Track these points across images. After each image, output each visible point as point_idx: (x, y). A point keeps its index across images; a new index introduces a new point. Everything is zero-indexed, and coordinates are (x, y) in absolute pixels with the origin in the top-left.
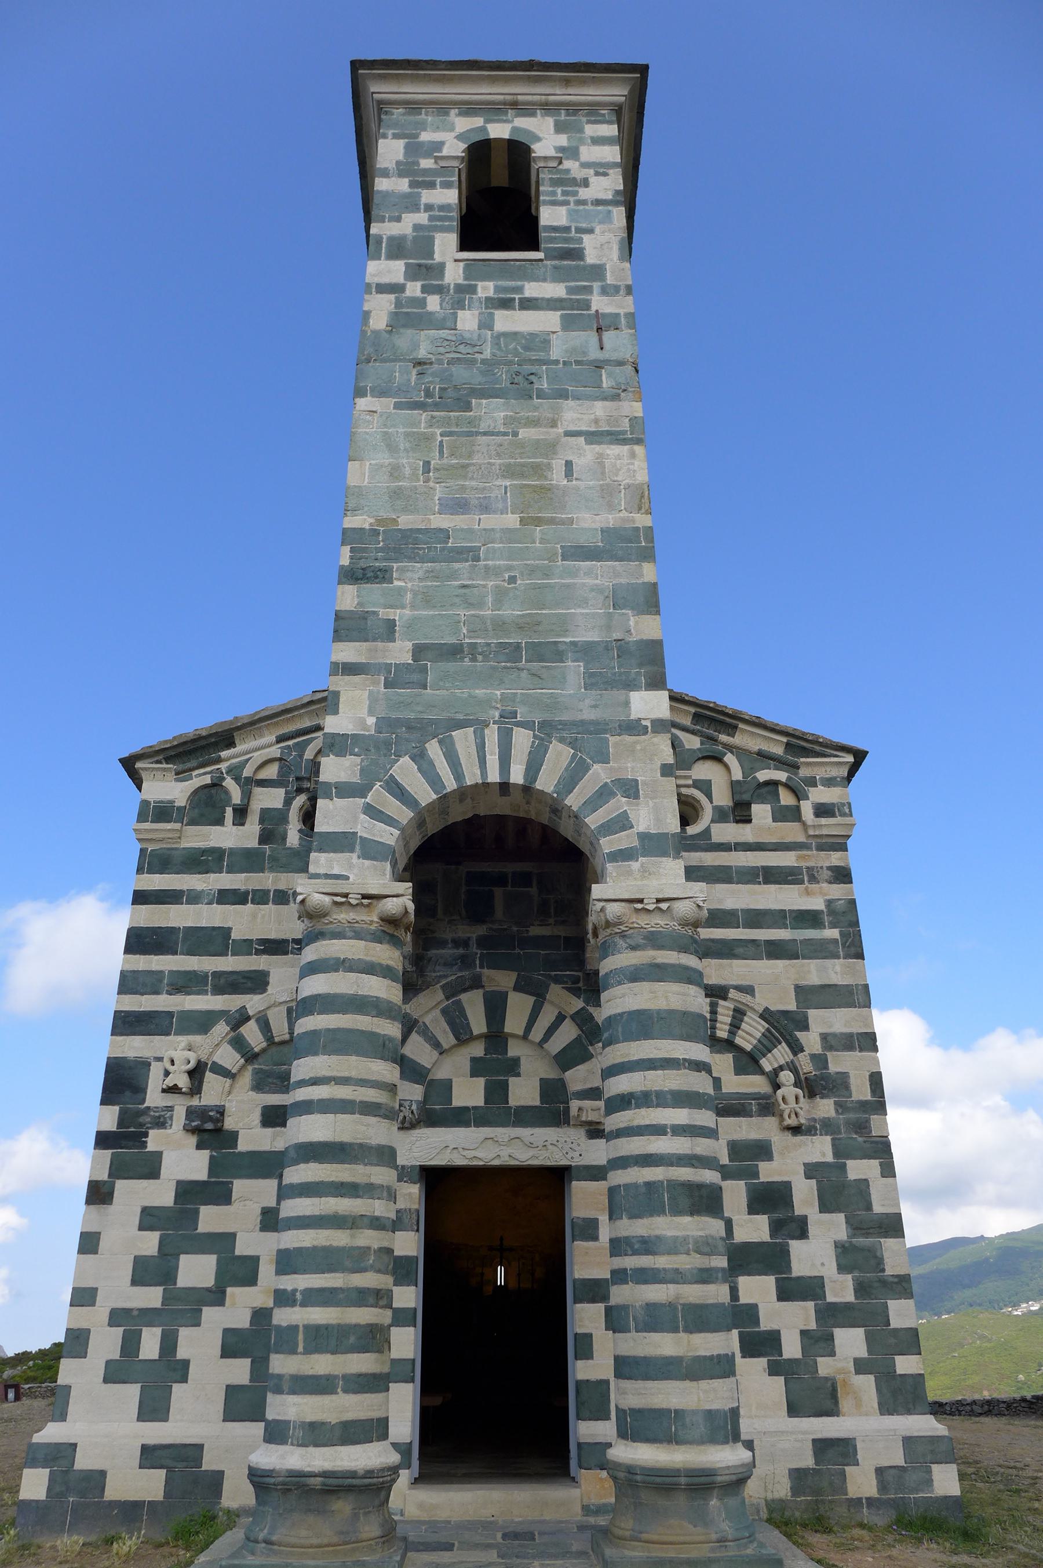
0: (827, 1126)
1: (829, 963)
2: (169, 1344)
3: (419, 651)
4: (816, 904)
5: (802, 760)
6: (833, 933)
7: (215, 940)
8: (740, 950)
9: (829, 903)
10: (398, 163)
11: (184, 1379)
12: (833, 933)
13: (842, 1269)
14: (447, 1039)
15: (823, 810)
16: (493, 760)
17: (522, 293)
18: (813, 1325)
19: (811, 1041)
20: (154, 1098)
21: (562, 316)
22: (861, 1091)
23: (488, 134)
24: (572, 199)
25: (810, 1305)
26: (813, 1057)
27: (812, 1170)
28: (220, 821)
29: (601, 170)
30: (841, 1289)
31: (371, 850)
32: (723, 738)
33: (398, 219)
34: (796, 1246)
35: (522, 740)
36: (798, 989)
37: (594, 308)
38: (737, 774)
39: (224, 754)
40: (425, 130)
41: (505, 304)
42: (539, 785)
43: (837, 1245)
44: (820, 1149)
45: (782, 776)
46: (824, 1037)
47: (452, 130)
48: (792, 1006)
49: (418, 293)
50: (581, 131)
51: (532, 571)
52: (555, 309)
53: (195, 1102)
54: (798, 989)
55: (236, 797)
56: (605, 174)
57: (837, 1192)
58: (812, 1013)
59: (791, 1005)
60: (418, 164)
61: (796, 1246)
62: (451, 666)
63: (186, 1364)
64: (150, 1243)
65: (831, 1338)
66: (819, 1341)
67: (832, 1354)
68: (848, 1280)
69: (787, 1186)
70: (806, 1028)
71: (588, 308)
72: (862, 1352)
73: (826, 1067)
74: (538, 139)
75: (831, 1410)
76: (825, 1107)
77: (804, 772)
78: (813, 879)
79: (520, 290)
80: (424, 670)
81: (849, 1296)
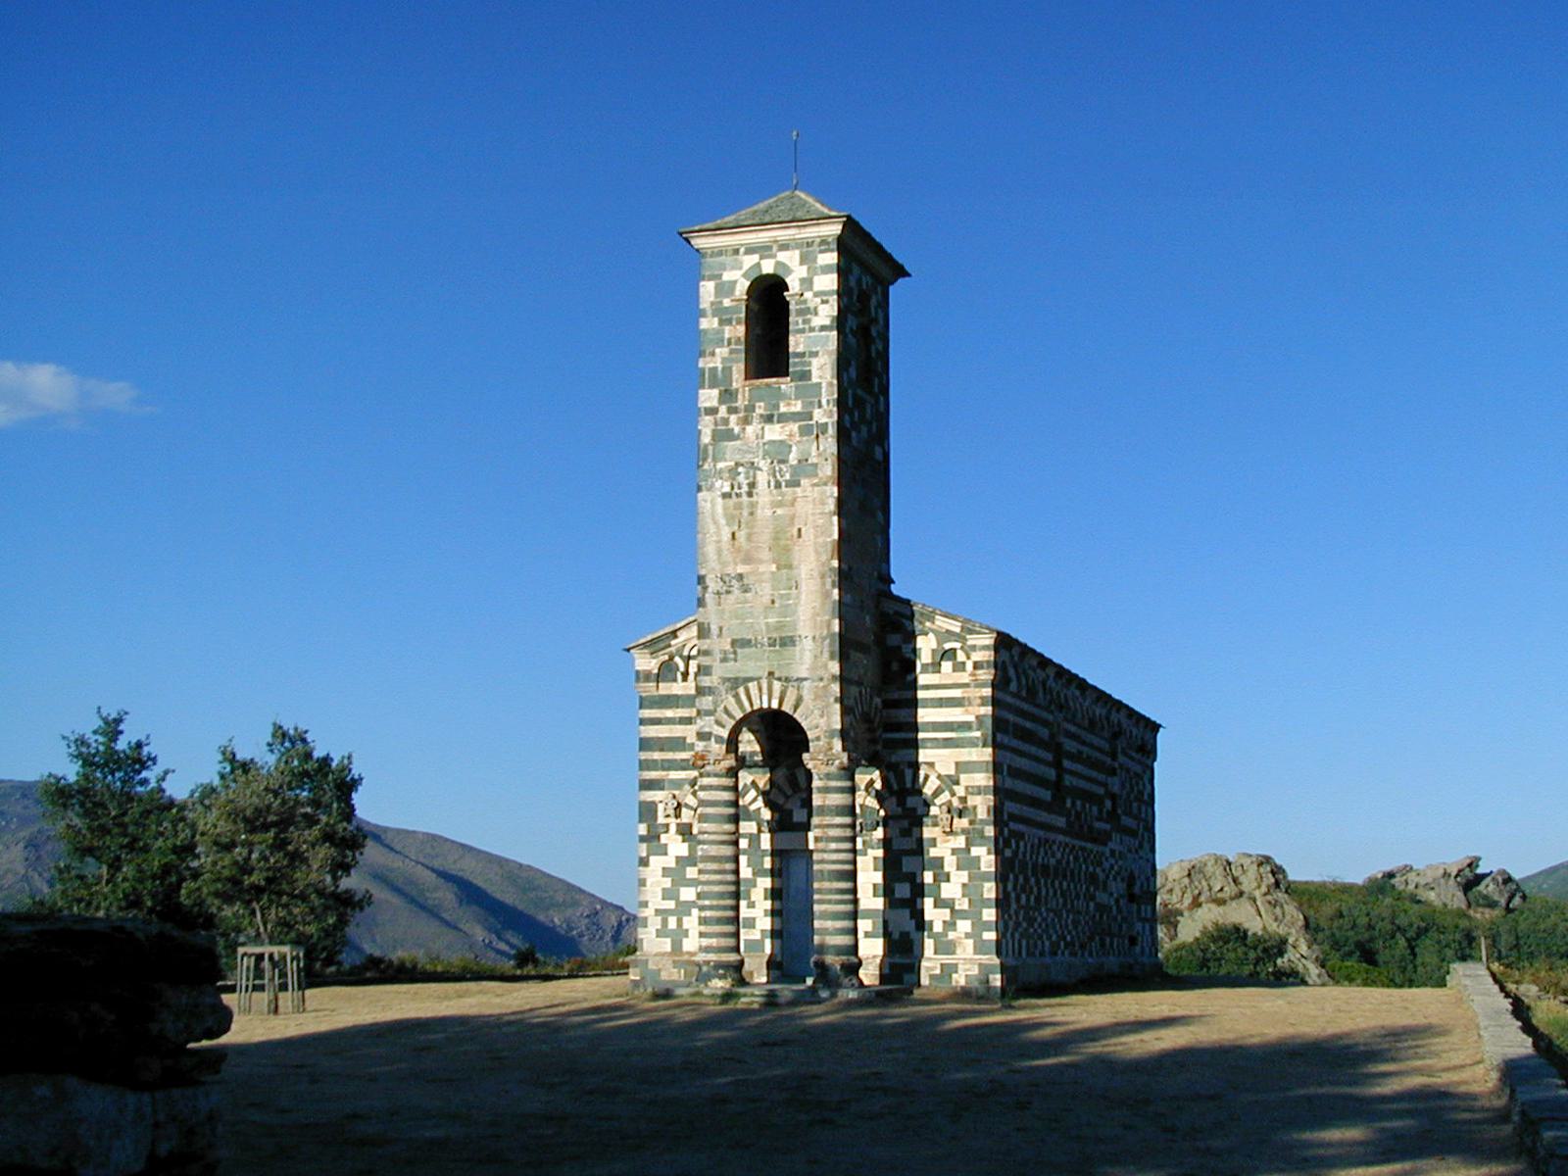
0: (964, 831)
1: (974, 750)
2: (680, 922)
3: (734, 643)
4: (971, 718)
5: (968, 637)
6: (978, 734)
7: (679, 744)
8: (929, 745)
9: (977, 717)
10: (712, 304)
11: (687, 936)
12: (978, 734)
13: (964, 896)
14: (789, 792)
15: (977, 666)
16: (765, 698)
17: (778, 409)
18: (948, 918)
19: (960, 791)
20: (661, 820)
21: (800, 427)
22: (982, 814)
23: (761, 270)
24: (807, 327)
25: (948, 911)
26: (960, 798)
27: (954, 851)
28: (675, 680)
29: (825, 298)
30: (963, 904)
31: (719, 739)
32: (928, 624)
33: (713, 354)
34: (944, 885)
35: (777, 686)
36: (957, 764)
37: (815, 419)
38: (935, 646)
39: (673, 642)
40: (725, 269)
41: (768, 419)
42: (784, 708)
43: (964, 885)
44: (960, 842)
45: (957, 645)
46: (967, 788)
47: (741, 268)
48: (953, 772)
49: (726, 416)
50: (815, 260)
51: (782, 596)
52: (795, 421)
53: (679, 821)
54: (957, 764)
55: (682, 668)
56: (826, 302)
57: (966, 862)
58: (963, 777)
59: (952, 772)
60: (721, 302)
61: (944, 885)
62: (747, 650)
63: (687, 930)
64: (667, 883)
65: (955, 924)
66: (950, 925)
67: (955, 930)
68: (966, 900)
69: (942, 859)
70: (957, 783)
71: (811, 419)
72: (969, 930)
73: (966, 802)
74: (789, 271)
75: (954, 953)
76: (962, 823)
77: (969, 643)
78: (970, 704)
79: (777, 407)
80: (735, 653)
81: (966, 907)
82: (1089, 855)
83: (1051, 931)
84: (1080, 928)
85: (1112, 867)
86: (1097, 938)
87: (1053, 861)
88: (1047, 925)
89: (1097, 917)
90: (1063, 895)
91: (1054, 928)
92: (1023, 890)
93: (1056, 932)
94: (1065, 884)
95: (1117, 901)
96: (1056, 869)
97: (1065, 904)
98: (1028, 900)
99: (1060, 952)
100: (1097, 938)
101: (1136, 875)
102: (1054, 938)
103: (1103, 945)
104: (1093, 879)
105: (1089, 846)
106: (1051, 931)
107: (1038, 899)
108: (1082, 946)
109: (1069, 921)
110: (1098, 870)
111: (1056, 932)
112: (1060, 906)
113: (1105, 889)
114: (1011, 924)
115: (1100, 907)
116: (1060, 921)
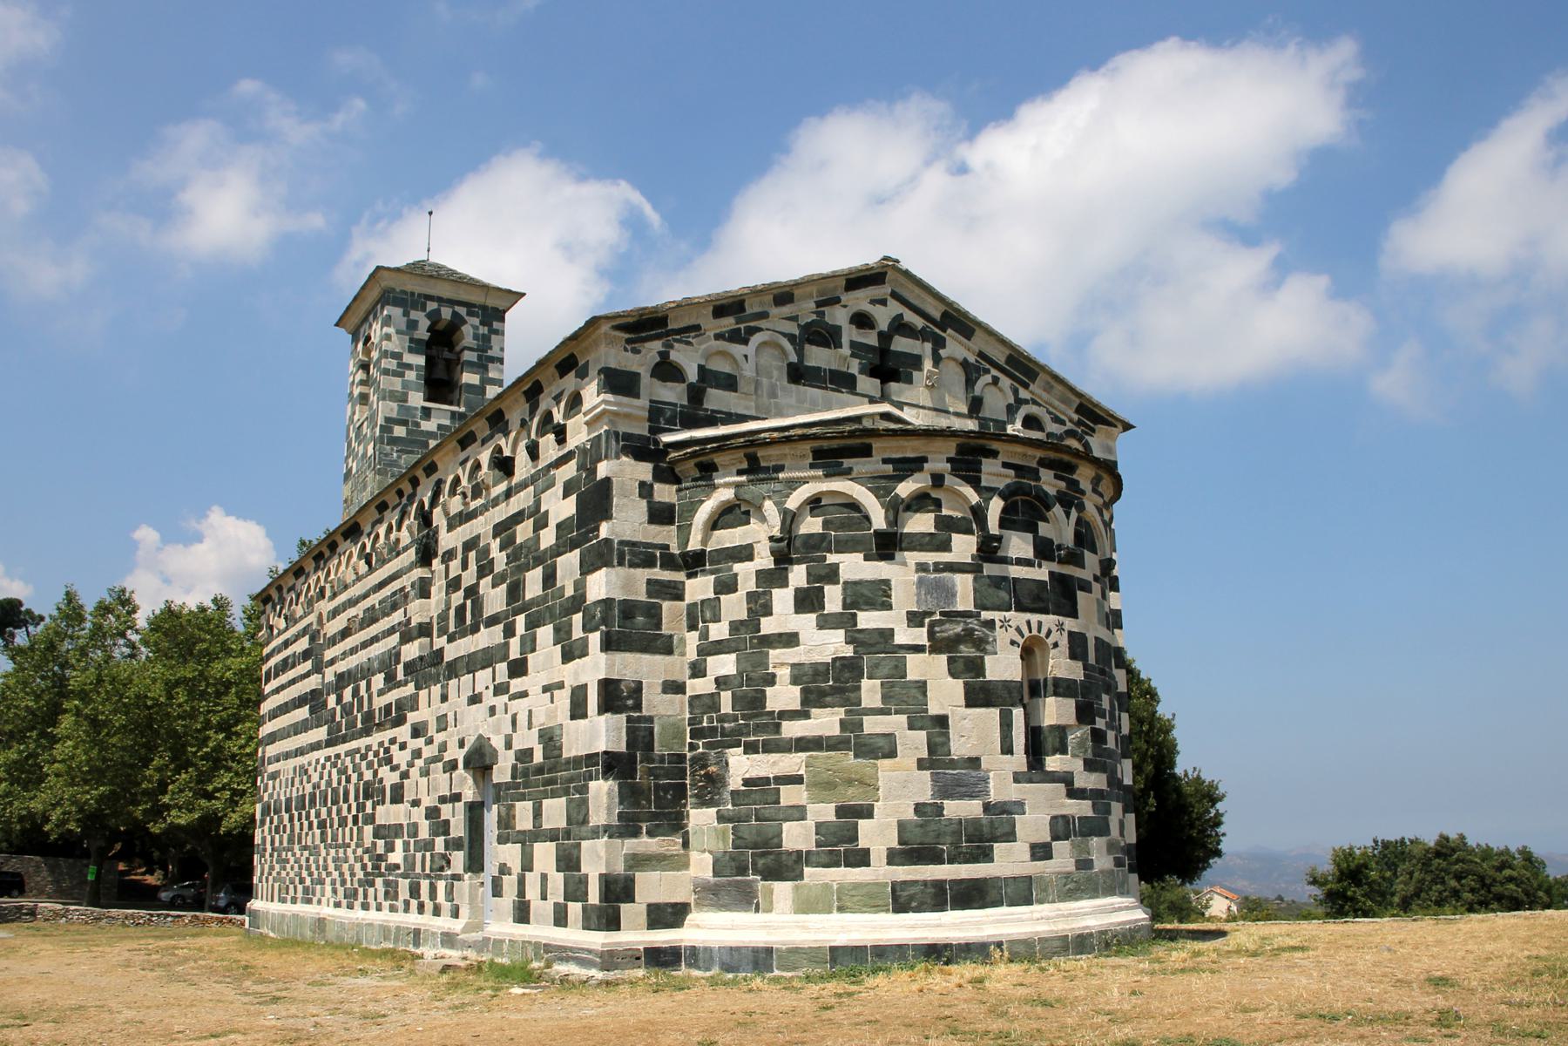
82: (364, 757)
83: (305, 873)
84: (345, 867)
85: (417, 754)
86: (379, 881)
87: (309, 788)
88: (300, 867)
89: (380, 850)
90: (322, 825)
91: (308, 868)
92: (277, 828)
93: (311, 874)
94: (324, 810)
95: (432, 813)
96: (313, 796)
97: (323, 834)
98: (281, 842)
99: (315, 900)
100: (379, 881)
101: (497, 742)
102: (308, 882)
103: (391, 894)
104: (372, 791)
105: (361, 743)
106: (305, 873)
107: (291, 841)
108: (351, 895)
109: (330, 859)
110: (384, 771)
111: (311, 874)
112: (318, 842)
113: (397, 797)
114: (267, 867)
115: (387, 833)
116: (317, 862)
